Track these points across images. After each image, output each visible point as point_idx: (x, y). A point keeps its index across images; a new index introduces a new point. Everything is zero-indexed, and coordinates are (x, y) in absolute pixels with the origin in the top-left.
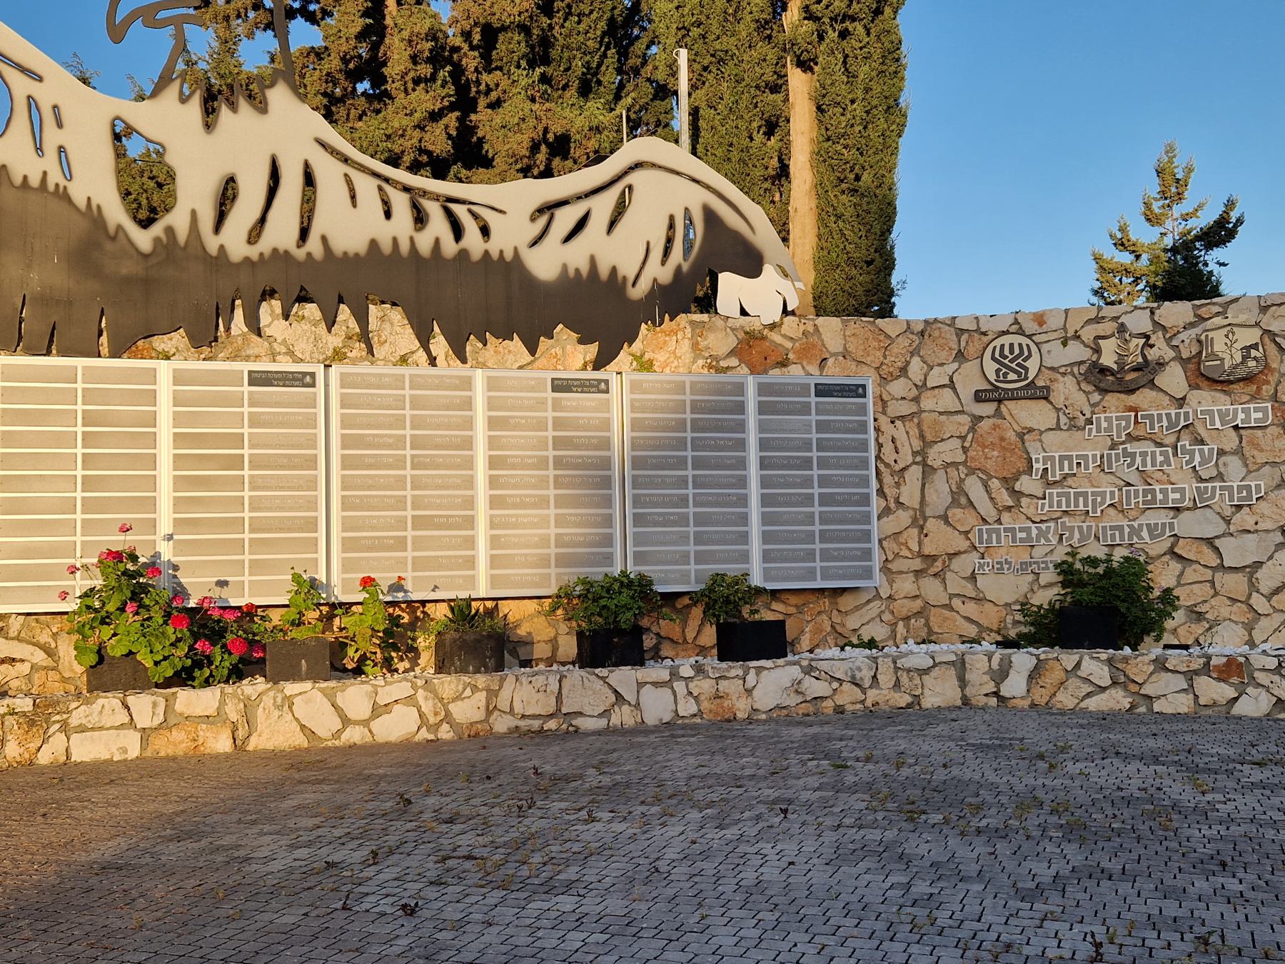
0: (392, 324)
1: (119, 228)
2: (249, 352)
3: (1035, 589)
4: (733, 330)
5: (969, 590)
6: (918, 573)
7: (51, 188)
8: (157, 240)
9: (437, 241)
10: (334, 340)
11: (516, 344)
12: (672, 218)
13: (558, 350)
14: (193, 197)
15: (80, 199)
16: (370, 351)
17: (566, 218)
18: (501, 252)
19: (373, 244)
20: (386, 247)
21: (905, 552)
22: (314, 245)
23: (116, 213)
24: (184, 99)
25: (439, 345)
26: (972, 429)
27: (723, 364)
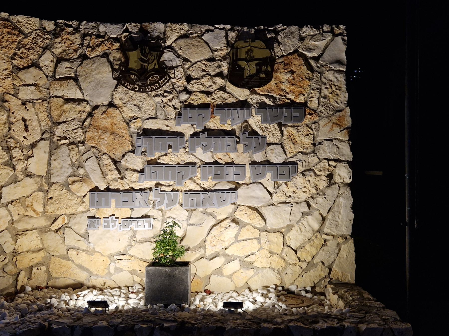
3: (133, 243)
5: (82, 244)
6: (43, 231)
21: (31, 213)
26: (90, 115)
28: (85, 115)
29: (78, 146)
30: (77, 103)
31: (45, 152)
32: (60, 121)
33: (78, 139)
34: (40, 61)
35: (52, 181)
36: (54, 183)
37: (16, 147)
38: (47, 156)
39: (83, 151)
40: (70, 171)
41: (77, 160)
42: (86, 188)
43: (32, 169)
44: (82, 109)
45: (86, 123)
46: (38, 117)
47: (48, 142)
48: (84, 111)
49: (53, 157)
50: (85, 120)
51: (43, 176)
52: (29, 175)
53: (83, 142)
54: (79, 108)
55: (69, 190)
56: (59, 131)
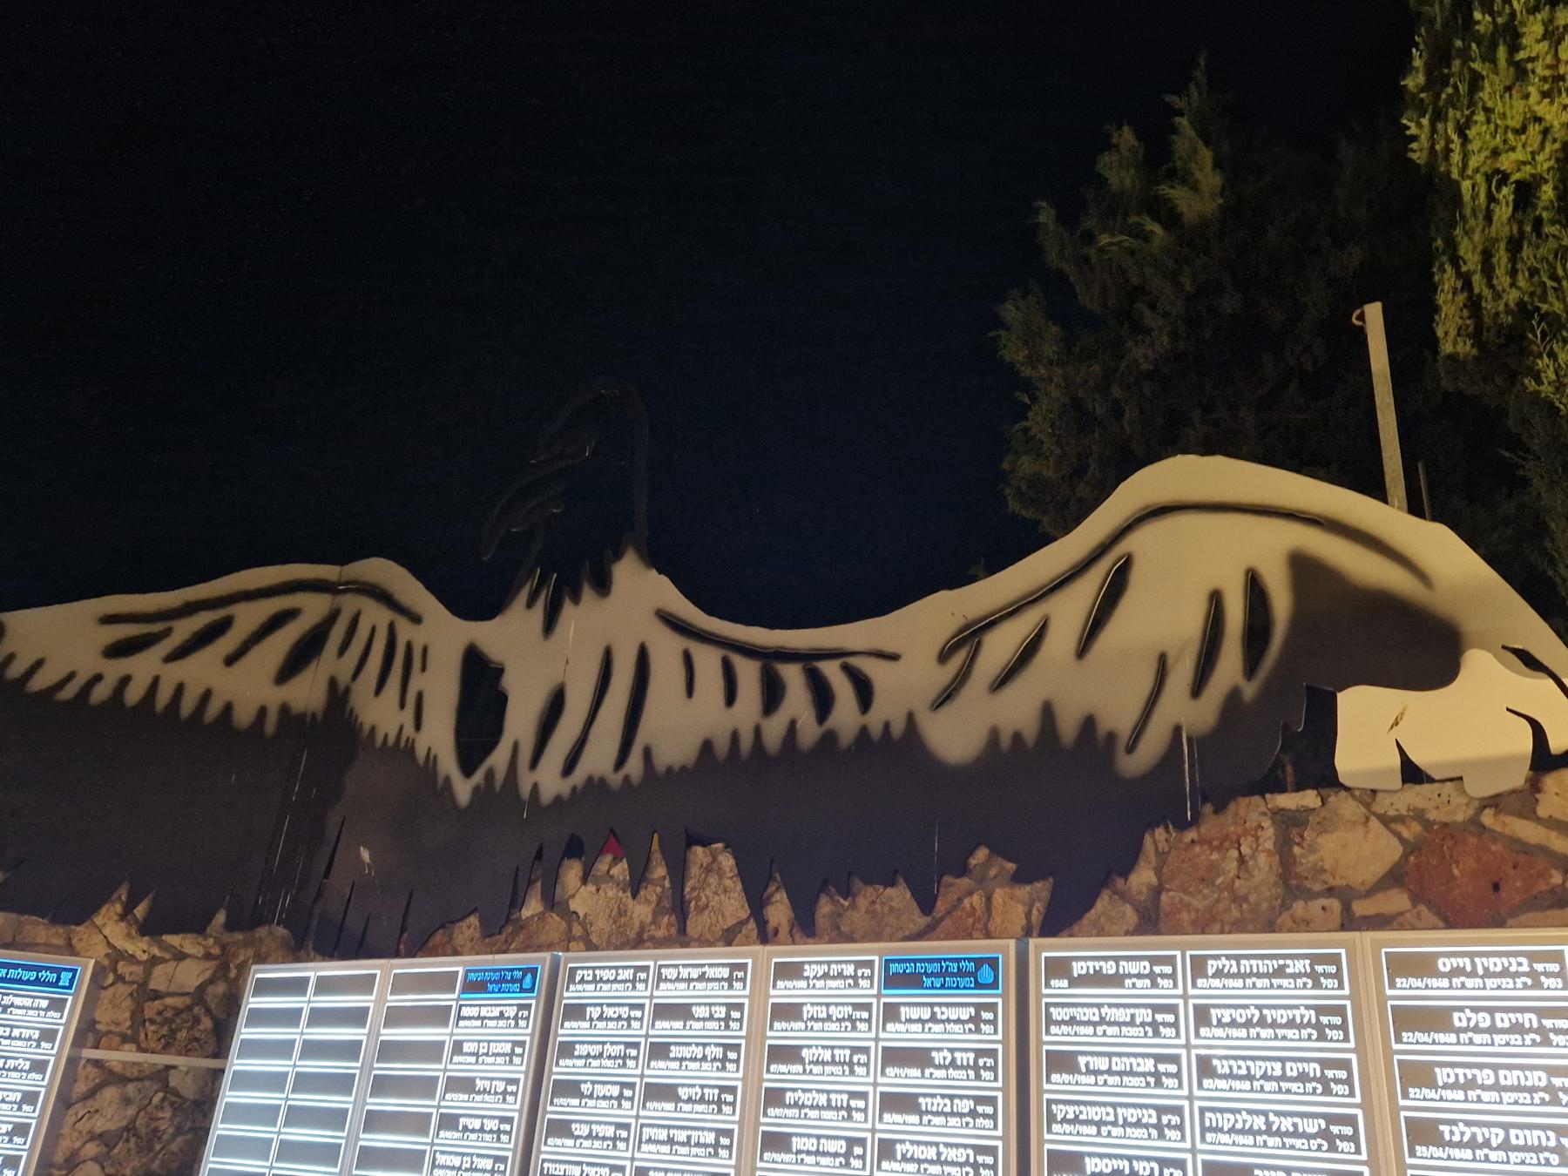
0: (721, 876)
1: (448, 779)
2: (543, 939)
4: (1386, 821)
7: (402, 744)
8: (476, 789)
9: (793, 723)
10: (641, 911)
11: (899, 896)
12: (1216, 600)
13: (977, 900)
14: (520, 722)
15: (421, 753)
16: (683, 930)
17: (1000, 646)
18: (887, 726)
19: (707, 746)
20: (722, 748)
22: (634, 765)
23: (448, 764)
24: (530, 603)
25: (779, 911)
27: (1360, 908)
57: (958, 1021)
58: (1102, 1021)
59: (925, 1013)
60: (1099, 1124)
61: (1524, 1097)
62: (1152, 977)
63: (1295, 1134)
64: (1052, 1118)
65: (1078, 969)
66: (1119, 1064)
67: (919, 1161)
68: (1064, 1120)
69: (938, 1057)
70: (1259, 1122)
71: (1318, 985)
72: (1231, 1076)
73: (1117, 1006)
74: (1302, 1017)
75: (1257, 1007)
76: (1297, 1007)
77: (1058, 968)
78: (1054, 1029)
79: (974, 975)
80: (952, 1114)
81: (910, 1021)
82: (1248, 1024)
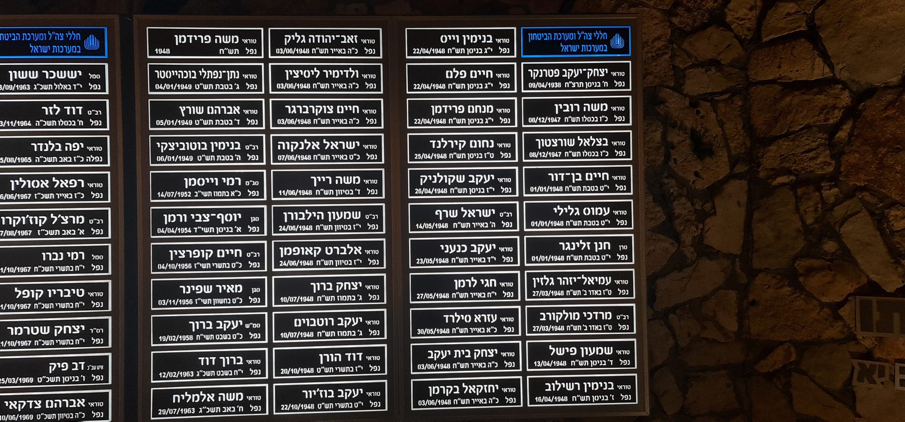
26: (851, 113)
28: (838, 114)
29: (819, 189)
30: (815, 90)
31: (739, 203)
32: (775, 132)
33: (819, 172)
34: (726, 10)
35: (756, 264)
36: (760, 271)
37: (681, 195)
38: (742, 211)
39: (832, 200)
40: (801, 244)
41: (817, 221)
42: (843, 287)
43: (714, 239)
44: (831, 101)
45: (842, 134)
46: (723, 130)
47: (744, 183)
48: (834, 107)
49: (756, 215)
50: (838, 127)
51: (736, 256)
52: (709, 253)
53: (834, 179)
54: (821, 100)
55: (799, 288)
56: (770, 157)
57: (66, 81)
58: (200, 79)
59: (34, 75)
60: (195, 154)
61: (480, 121)
62: (242, 48)
63: (341, 151)
64: (157, 152)
65: (179, 39)
66: (211, 110)
67: (32, 191)
68: (168, 152)
69: (48, 110)
70: (316, 145)
71: (362, 53)
72: (298, 116)
73: (212, 68)
74: (350, 74)
75: (318, 67)
76: (347, 68)
77: (163, 40)
78: (157, 86)
79: (81, 43)
80: (64, 153)
81: (19, 81)
82: (312, 80)
